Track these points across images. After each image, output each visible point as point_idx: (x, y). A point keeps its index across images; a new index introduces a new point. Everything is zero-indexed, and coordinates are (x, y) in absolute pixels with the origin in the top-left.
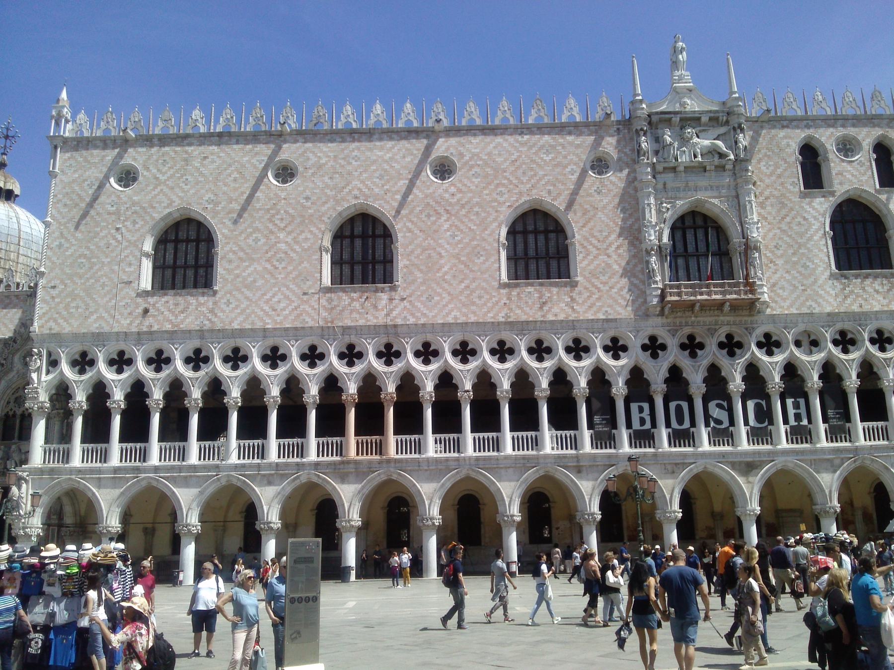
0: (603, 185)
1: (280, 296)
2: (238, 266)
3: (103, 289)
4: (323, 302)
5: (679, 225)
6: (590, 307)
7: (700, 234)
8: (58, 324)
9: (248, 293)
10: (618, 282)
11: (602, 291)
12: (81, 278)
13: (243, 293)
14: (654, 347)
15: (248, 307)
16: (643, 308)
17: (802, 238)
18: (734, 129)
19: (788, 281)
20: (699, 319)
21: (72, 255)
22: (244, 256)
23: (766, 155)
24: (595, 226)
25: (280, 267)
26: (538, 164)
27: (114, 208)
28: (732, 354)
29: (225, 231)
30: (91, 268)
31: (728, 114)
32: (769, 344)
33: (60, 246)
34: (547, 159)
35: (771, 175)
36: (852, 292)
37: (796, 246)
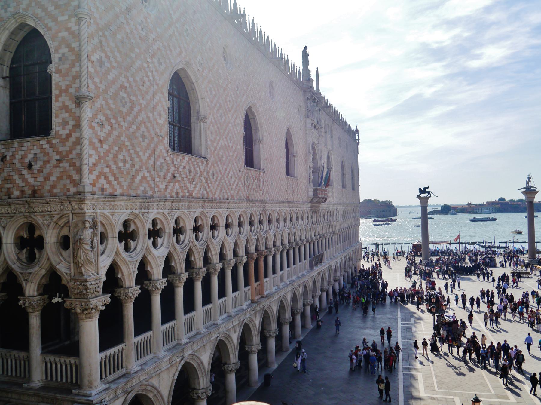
1: (231, 173)
2: (215, 139)
3: (144, 141)
4: (245, 180)
8: (109, 182)
9: (220, 166)
12: (124, 120)
13: (218, 165)
15: (221, 179)
21: (114, 82)
22: (217, 130)
25: (231, 144)
27: (144, 33)
29: (208, 100)
30: (132, 108)
33: (101, 62)
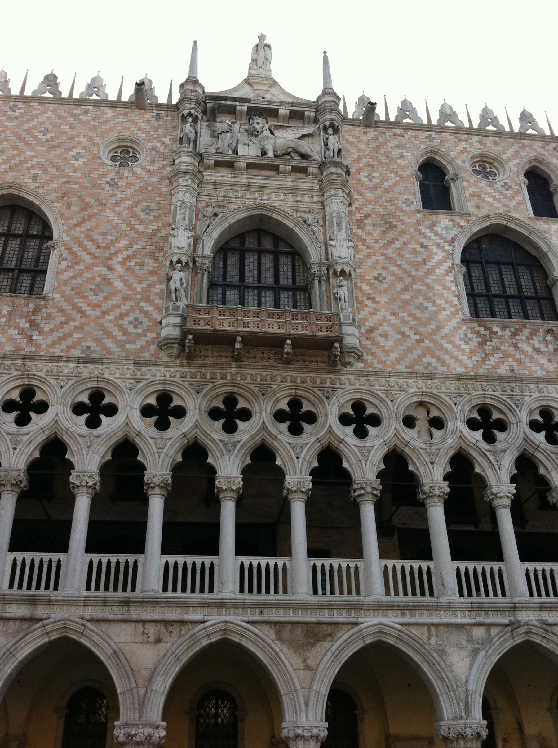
0: (122, 177)
5: (236, 244)
6: (60, 339)
7: (267, 261)
10: (118, 306)
11: (88, 317)
14: (163, 411)
16: (153, 347)
17: (417, 270)
18: (325, 129)
19: (394, 326)
20: (244, 371)
23: (368, 165)
24: (96, 227)
26: (27, 144)
28: (296, 430)
31: (317, 112)
32: (360, 419)
34: (44, 138)
35: (375, 188)
36: (497, 349)
37: (408, 280)
